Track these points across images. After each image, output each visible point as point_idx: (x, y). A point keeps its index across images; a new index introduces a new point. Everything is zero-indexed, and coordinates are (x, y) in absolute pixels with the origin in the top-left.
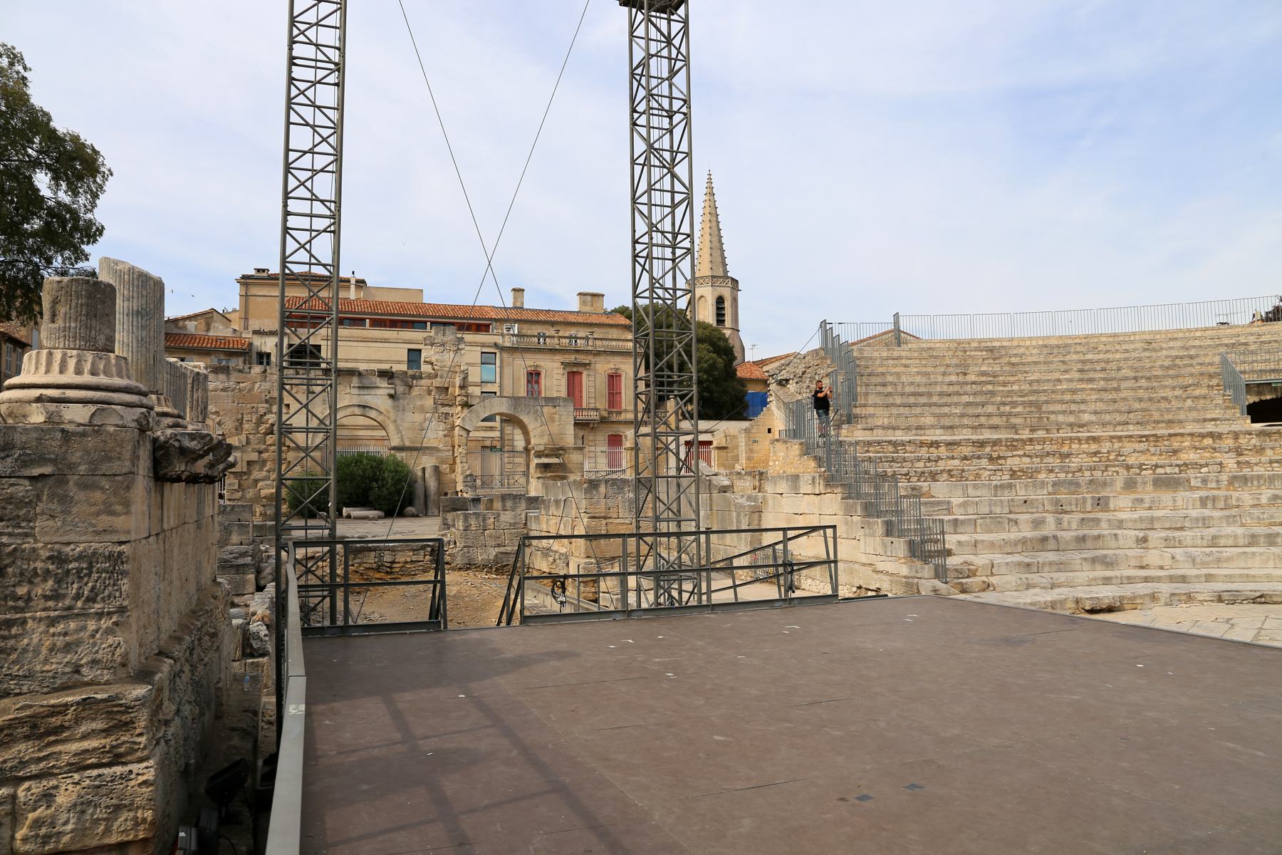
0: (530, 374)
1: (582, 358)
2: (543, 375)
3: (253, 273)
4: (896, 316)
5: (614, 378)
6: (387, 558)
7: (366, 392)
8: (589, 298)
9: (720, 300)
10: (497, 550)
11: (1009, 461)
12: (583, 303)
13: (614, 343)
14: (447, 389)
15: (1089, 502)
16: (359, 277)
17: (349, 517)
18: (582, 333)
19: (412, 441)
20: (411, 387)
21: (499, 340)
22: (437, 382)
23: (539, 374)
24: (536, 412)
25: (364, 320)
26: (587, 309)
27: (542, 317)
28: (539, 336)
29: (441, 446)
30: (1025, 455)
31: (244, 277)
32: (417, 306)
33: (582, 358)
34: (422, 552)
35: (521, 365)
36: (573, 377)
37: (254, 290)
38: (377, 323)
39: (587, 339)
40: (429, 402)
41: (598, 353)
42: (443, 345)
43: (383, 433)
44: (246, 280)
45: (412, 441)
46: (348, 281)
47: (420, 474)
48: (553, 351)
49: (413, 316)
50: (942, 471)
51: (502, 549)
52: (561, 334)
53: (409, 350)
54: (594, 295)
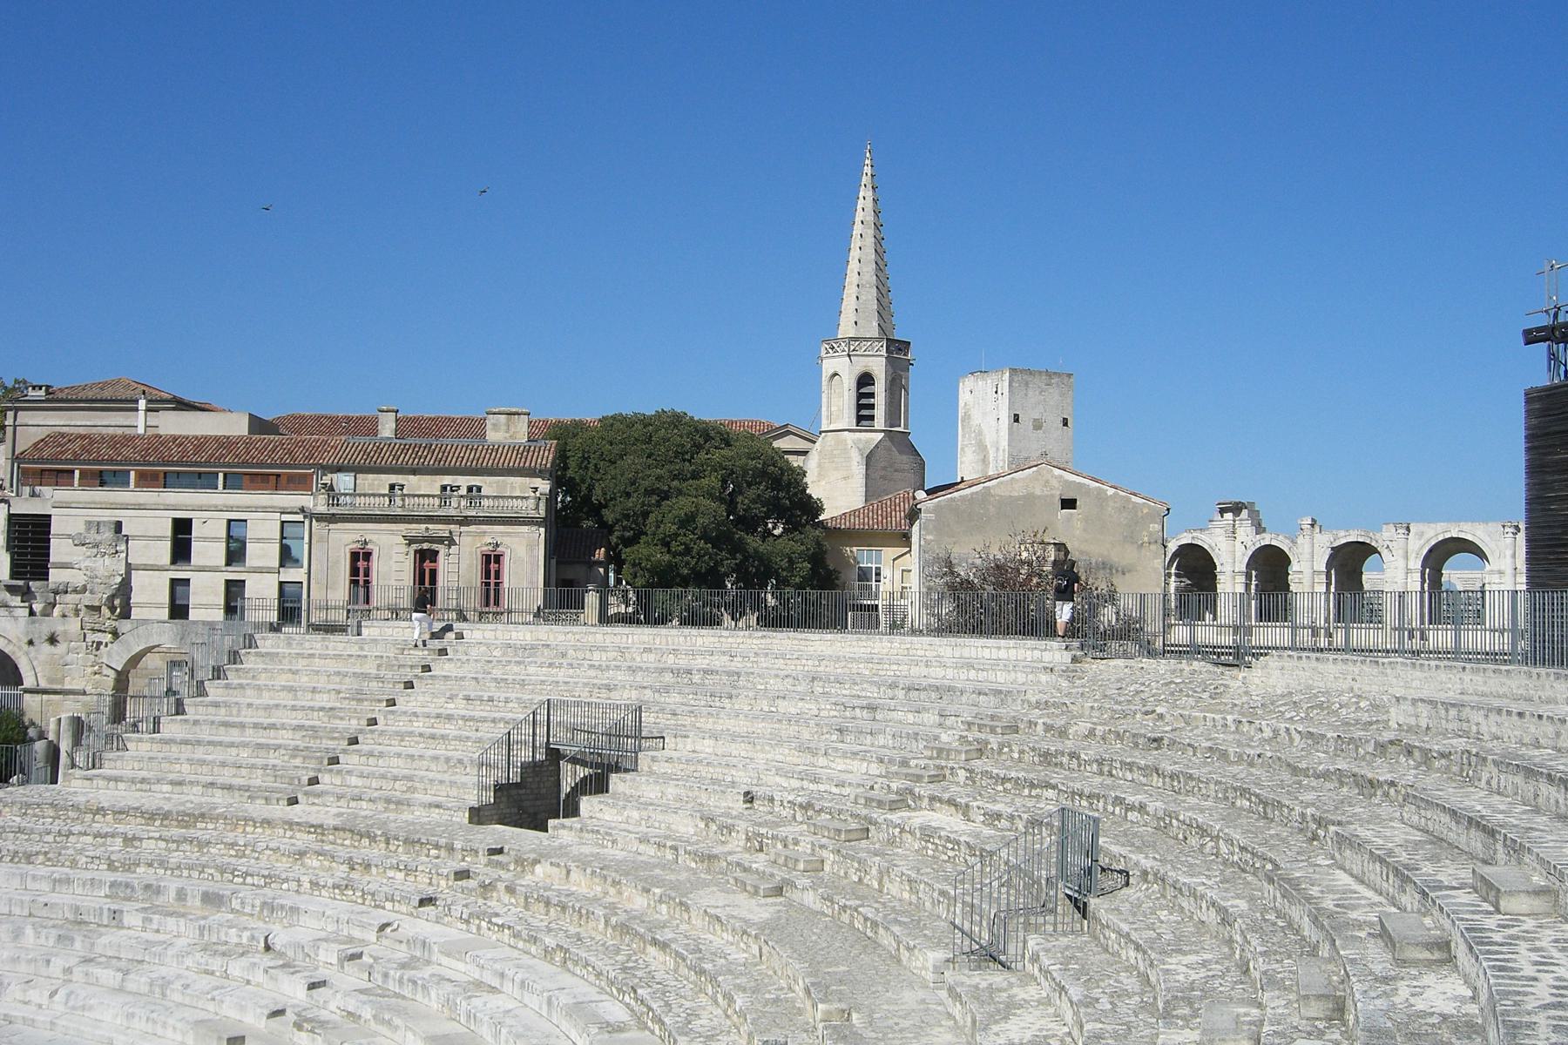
2: (375, 557)
4: (1531, 337)
5: (492, 562)
9: (865, 380)
11: (145, 844)
13: (511, 503)
15: (106, 913)
22: (87, 599)
23: (368, 556)
29: (89, 689)
30: (160, 838)
36: (425, 558)
40: (73, 625)
42: (96, 546)
45: (51, 681)
47: (53, 726)
50: (37, 853)
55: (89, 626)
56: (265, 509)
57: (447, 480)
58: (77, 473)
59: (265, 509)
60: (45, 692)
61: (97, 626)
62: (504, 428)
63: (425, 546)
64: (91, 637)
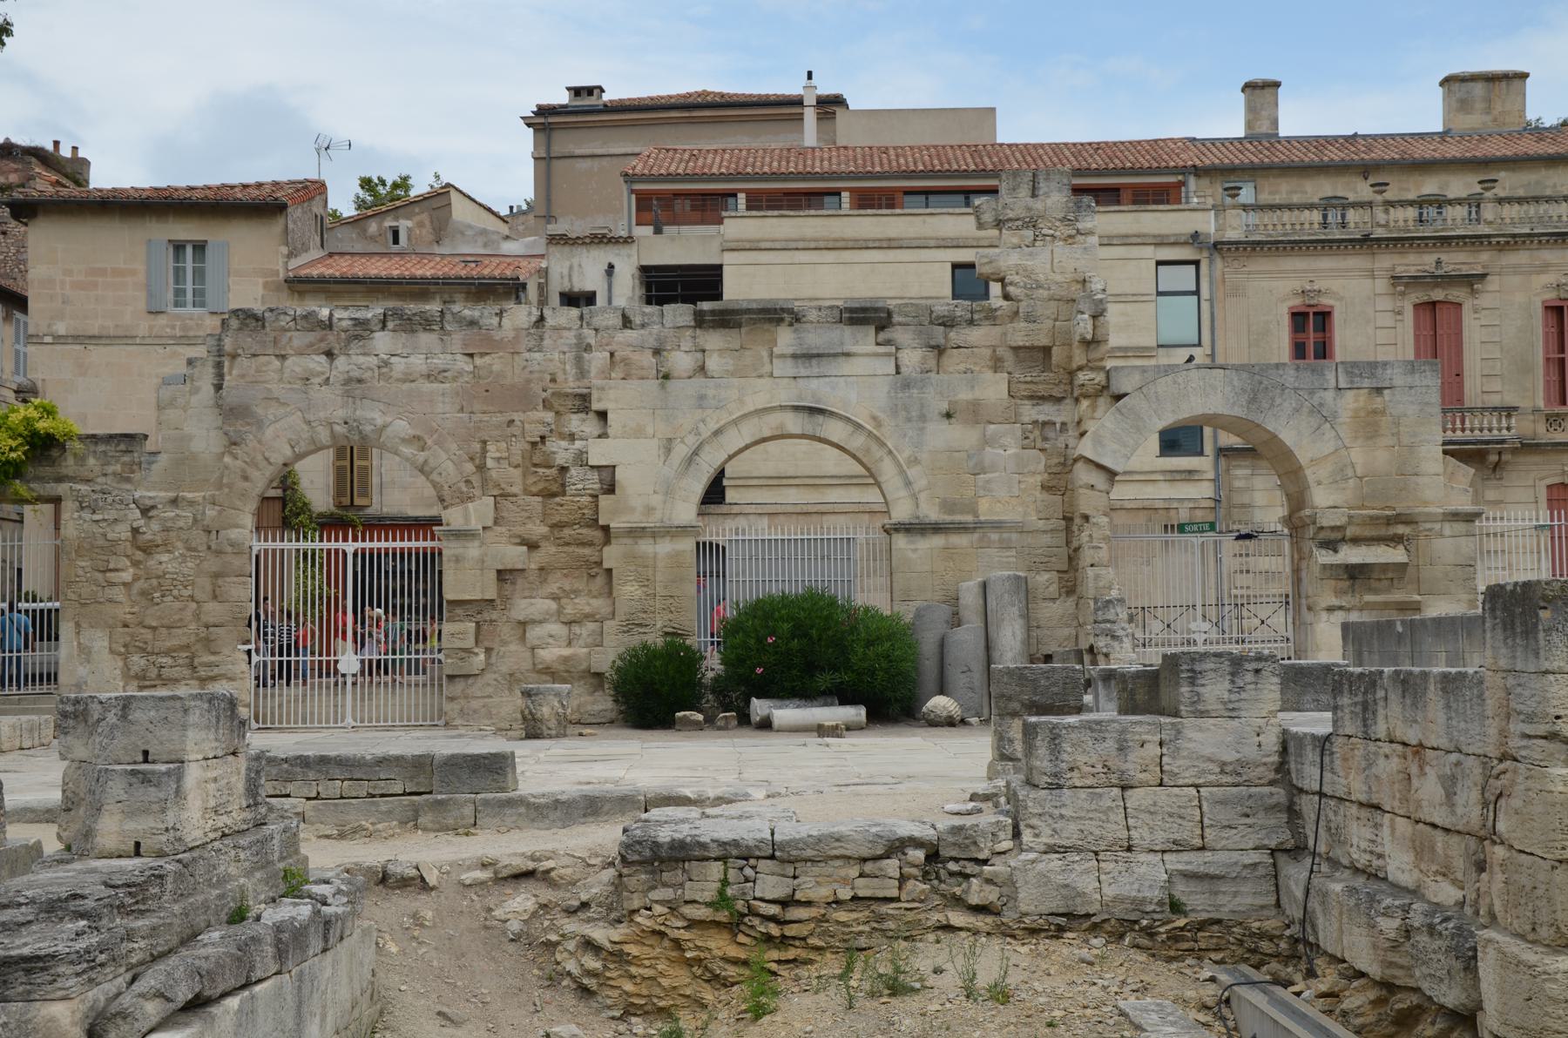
0: (1298, 318)
1: (1456, 261)
2: (1337, 318)
3: (563, 98)
6: (770, 885)
7: (815, 368)
8: (1479, 89)
10: (1175, 862)
12: (1464, 105)
14: (1047, 351)
16: (826, 88)
17: (766, 725)
18: (1460, 185)
19: (948, 506)
20: (940, 350)
21: (1207, 224)
22: (1019, 334)
23: (1324, 317)
24: (1317, 410)
25: (837, 193)
26: (1473, 121)
27: (1333, 154)
28: (1327, 204)
31: (543, 111)
32: (975, 150)
33: (1456, 261)
34: (892, 866)
35: (1273, 290)
37: (565, 143)
38: (867, 200)
39: (1474, 202)
41: (1514, 242)
43: (872, 496)
44: (545, 120)
45: (948, 506)
46: (798, 102)
48: (1366, 243)
49: (965, 174)
51: (1194, 862)
52: (1390, 195)
53: (956, 266)
54: (1491, 79)
55: (1023, 390)
56: (1126, 240)
57: (1430, 186)
58: (742, 197)
59: (1126, 240)
60: (937, 528)
61: (1042, 390)
62: (1479, 105)
63: (1438, 295)
64: (1030, 412)
